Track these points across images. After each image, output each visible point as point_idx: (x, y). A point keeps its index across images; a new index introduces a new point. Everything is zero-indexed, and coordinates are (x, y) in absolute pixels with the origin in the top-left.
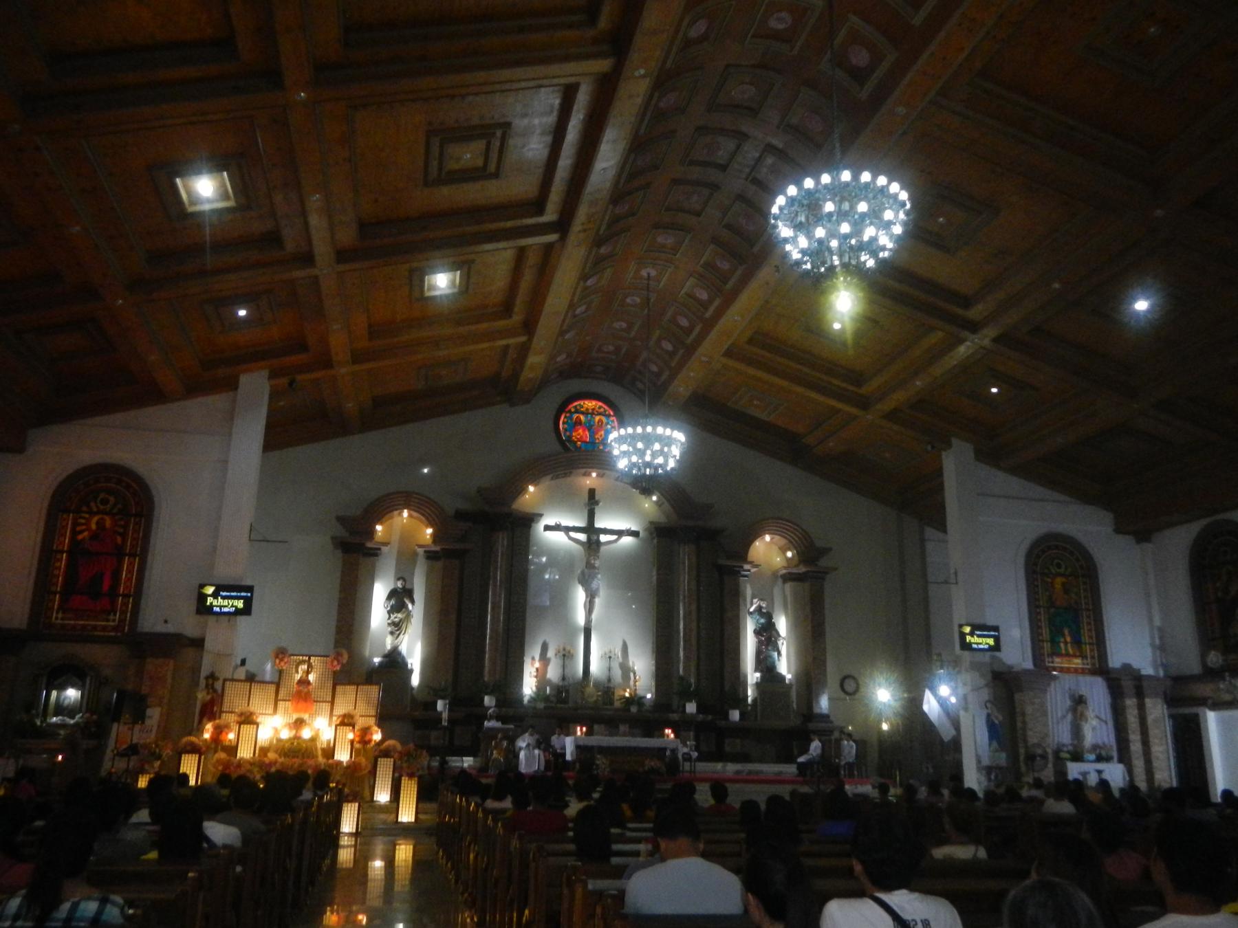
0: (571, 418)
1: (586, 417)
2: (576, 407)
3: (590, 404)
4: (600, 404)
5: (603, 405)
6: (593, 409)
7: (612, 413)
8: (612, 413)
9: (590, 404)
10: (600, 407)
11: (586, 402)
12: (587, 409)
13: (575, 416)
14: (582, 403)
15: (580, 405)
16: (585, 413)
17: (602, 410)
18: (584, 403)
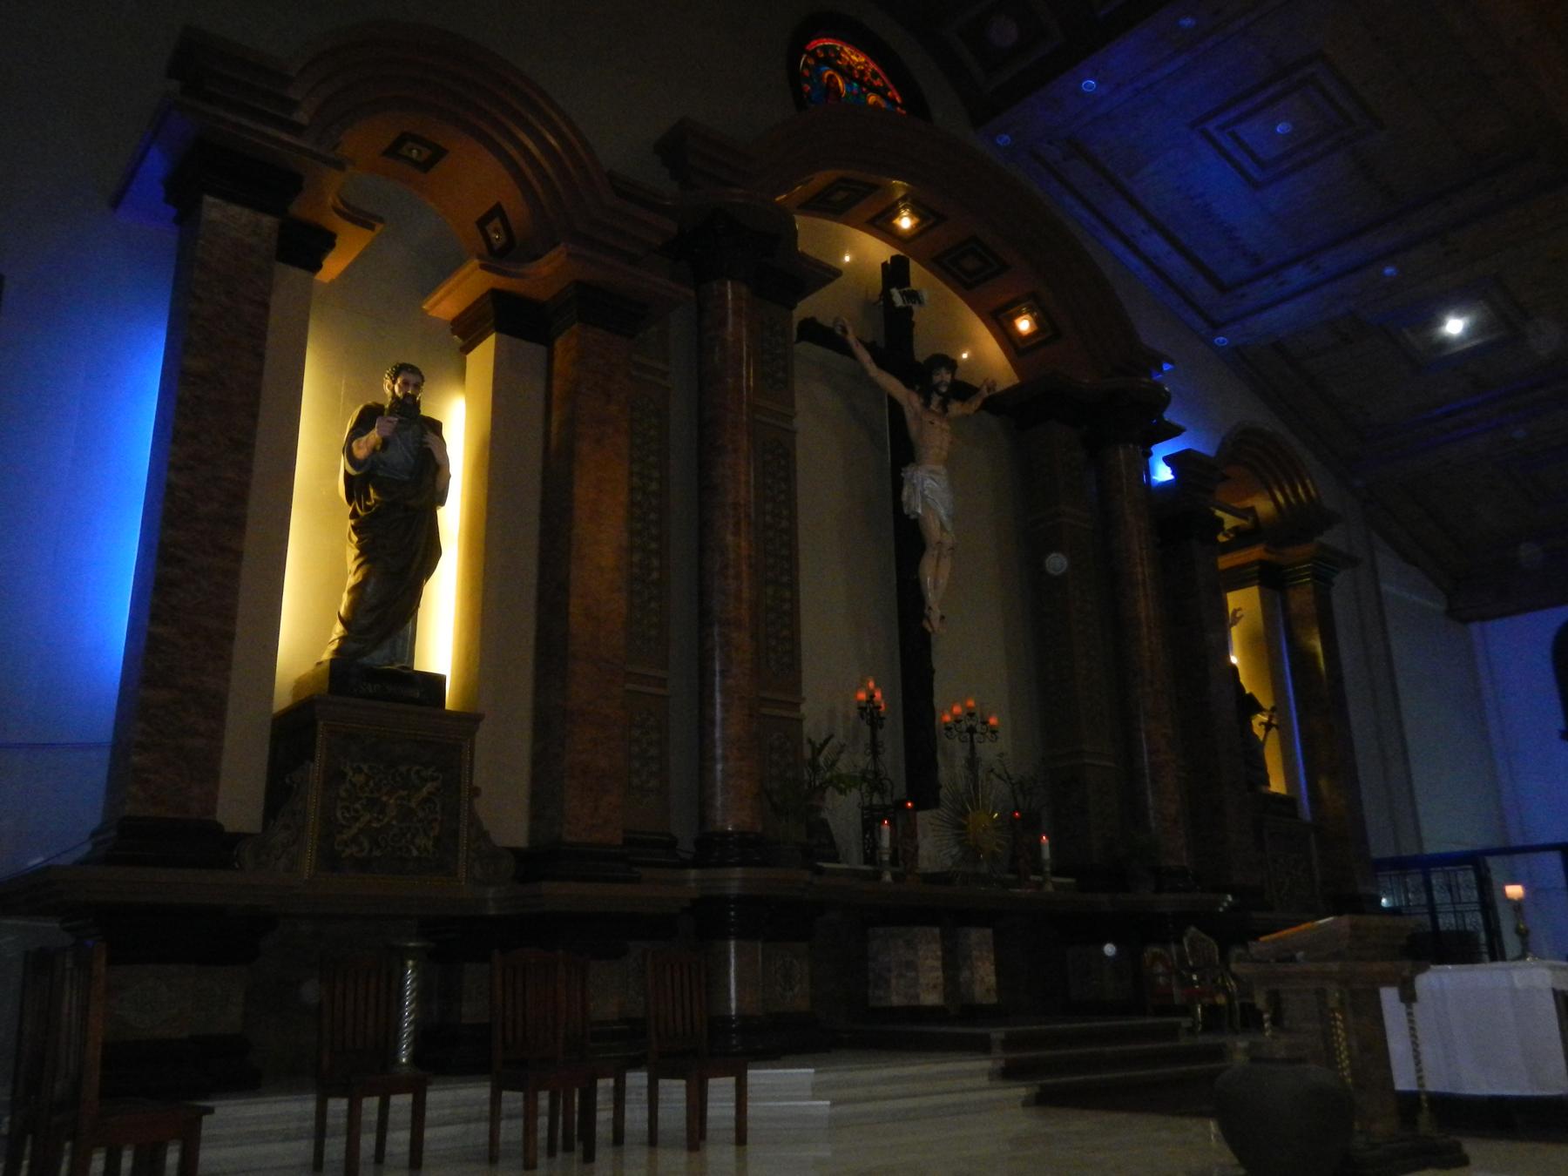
0: (820, 77)
1: (848, 84)
2: (824, 48)
3: (854, 57)
4: (872, 66)
5: (881, 73)
6: (862, 73)
7: (898, 100)
8: (898, 100)
9: (854, 57)
10: (875, 75)
11: (846, 49)
12: (850, 67)
13: (828, 73)
14: (838, 45)
15: (833, 48)
16: (848, 72)
17: (878, 82)
18: (842, 48)
